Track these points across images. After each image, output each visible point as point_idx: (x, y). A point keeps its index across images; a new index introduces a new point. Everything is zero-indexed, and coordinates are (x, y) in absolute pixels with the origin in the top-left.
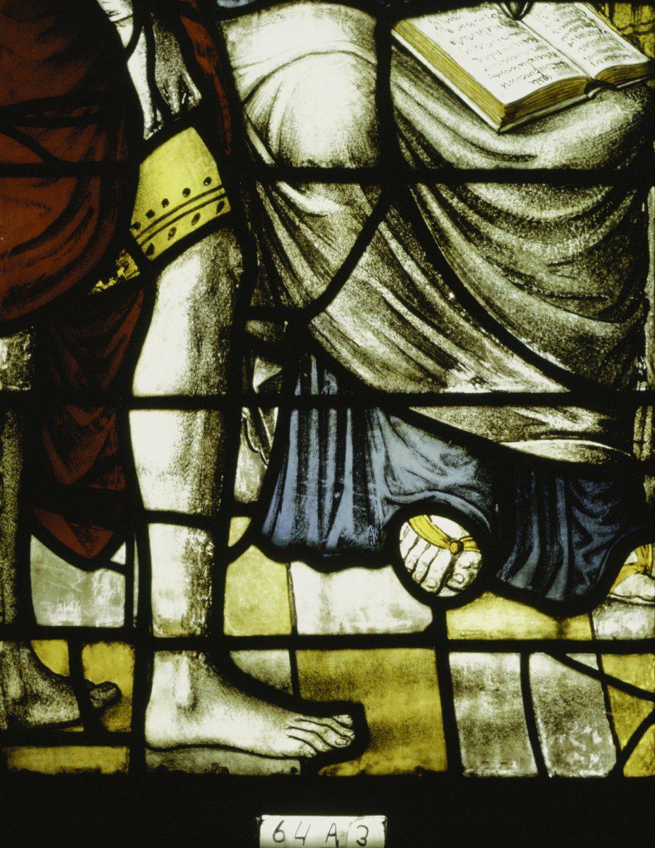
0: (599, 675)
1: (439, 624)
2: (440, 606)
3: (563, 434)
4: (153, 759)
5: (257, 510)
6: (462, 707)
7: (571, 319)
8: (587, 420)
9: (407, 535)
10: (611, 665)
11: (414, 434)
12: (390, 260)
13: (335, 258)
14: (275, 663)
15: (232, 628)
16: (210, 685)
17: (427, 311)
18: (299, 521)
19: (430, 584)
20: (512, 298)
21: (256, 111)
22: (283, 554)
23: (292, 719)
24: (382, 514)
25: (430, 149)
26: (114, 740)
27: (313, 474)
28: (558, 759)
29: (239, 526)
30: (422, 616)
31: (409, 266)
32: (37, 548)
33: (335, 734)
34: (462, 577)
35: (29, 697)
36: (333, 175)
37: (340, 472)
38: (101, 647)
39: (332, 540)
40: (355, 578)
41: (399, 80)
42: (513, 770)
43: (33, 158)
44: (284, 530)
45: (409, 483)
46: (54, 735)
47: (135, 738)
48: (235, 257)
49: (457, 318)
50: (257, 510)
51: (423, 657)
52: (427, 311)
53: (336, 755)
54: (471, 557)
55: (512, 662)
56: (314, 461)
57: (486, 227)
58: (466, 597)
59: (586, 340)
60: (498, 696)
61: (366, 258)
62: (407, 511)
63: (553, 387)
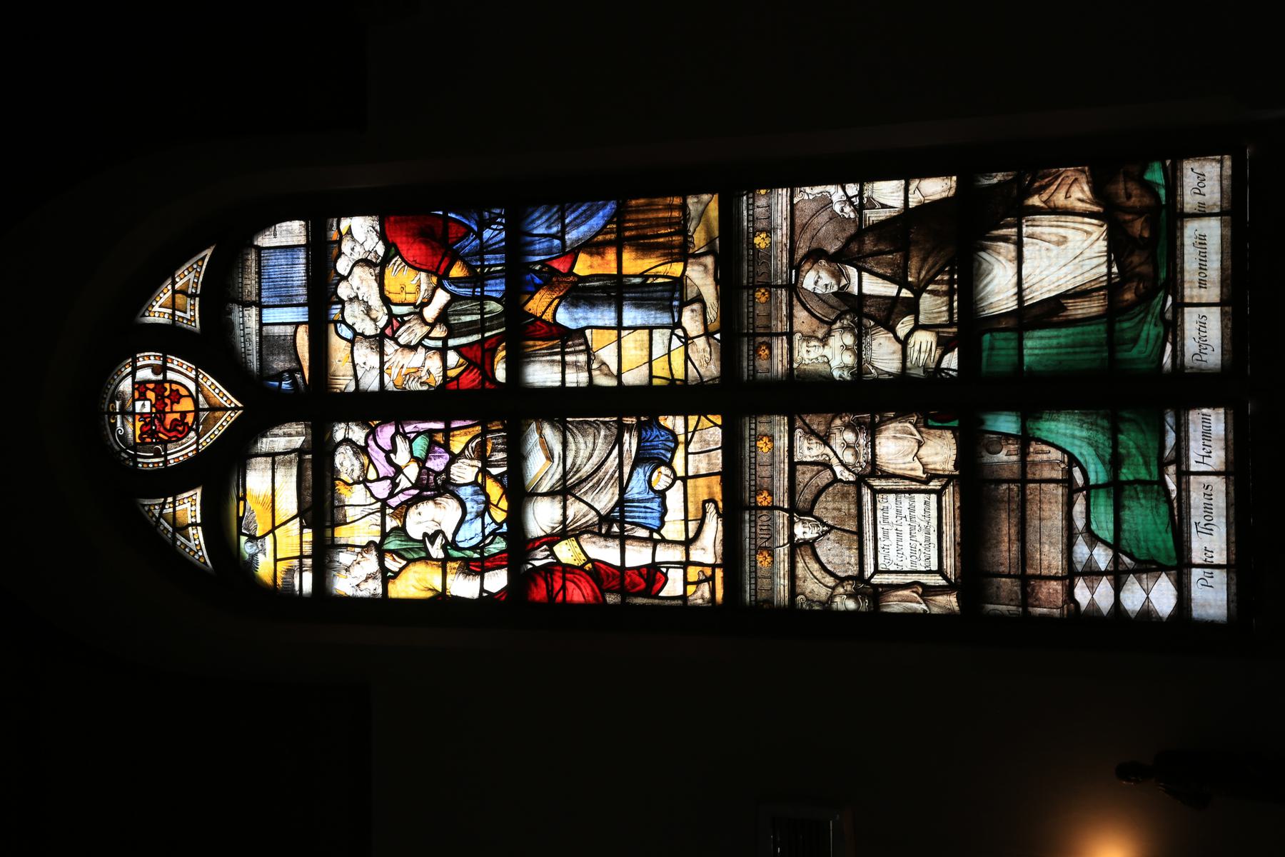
0: (694, 432)
1: (681, 478)
2: (676, 478)
3: (630, 443)
4: (719, 561)
5: (652, 531)
6: (703, 472)
7: (600, 441)
8: (626, 436)
9: (657, 488)
10: (691, 429)
11: (631, 485)
12: (586, 493)
13: (586, 508)
14: (693, 526)
15: (683, 538)
16: (699, 544)
17: (599, 482)
18: (653, 518)
19: (670, 481)
20: (595, 460)
21: (549, 531)
22: (663, 523)
23: (707, 521)
24: (652, 495)
25: (558, 482)
26: (714, 572)
27: (641, 515)
28: (717, 444)
29: (656, 536)
30: (679, 483)
31: (587, 488)
32: (661, 594)
33: (711, 508)
34: (668, 472)
35: (703, 598)
36: (565, 508)
37: (641, 507)
38: (688, 576)
39: (659, 509)
40: (669, 503)
41: (539, 491)
42: (720, 456)
43: (561, 592)
44: (657, 523)
45: (643, 486)
46: (713, 591)
47: (713, 566)
48: (586, 536)
49: (601, 474)
50: (652, 531)
51: (690, 482)
52: (599, 482)
53: (717, 507)
54: (663, 469)
55: (690, 457)
56: (637, 514)
57: (577, 466)
58: (674, 472)
59: (606, 437)
60: (700, 461)
61: (585, 498)
62: (651, 487)
63: (617, 447)
